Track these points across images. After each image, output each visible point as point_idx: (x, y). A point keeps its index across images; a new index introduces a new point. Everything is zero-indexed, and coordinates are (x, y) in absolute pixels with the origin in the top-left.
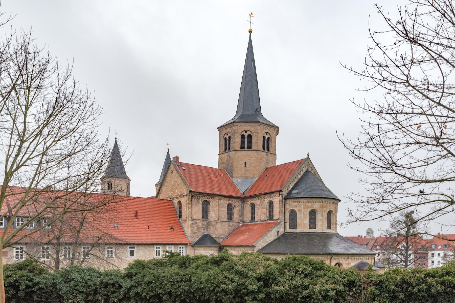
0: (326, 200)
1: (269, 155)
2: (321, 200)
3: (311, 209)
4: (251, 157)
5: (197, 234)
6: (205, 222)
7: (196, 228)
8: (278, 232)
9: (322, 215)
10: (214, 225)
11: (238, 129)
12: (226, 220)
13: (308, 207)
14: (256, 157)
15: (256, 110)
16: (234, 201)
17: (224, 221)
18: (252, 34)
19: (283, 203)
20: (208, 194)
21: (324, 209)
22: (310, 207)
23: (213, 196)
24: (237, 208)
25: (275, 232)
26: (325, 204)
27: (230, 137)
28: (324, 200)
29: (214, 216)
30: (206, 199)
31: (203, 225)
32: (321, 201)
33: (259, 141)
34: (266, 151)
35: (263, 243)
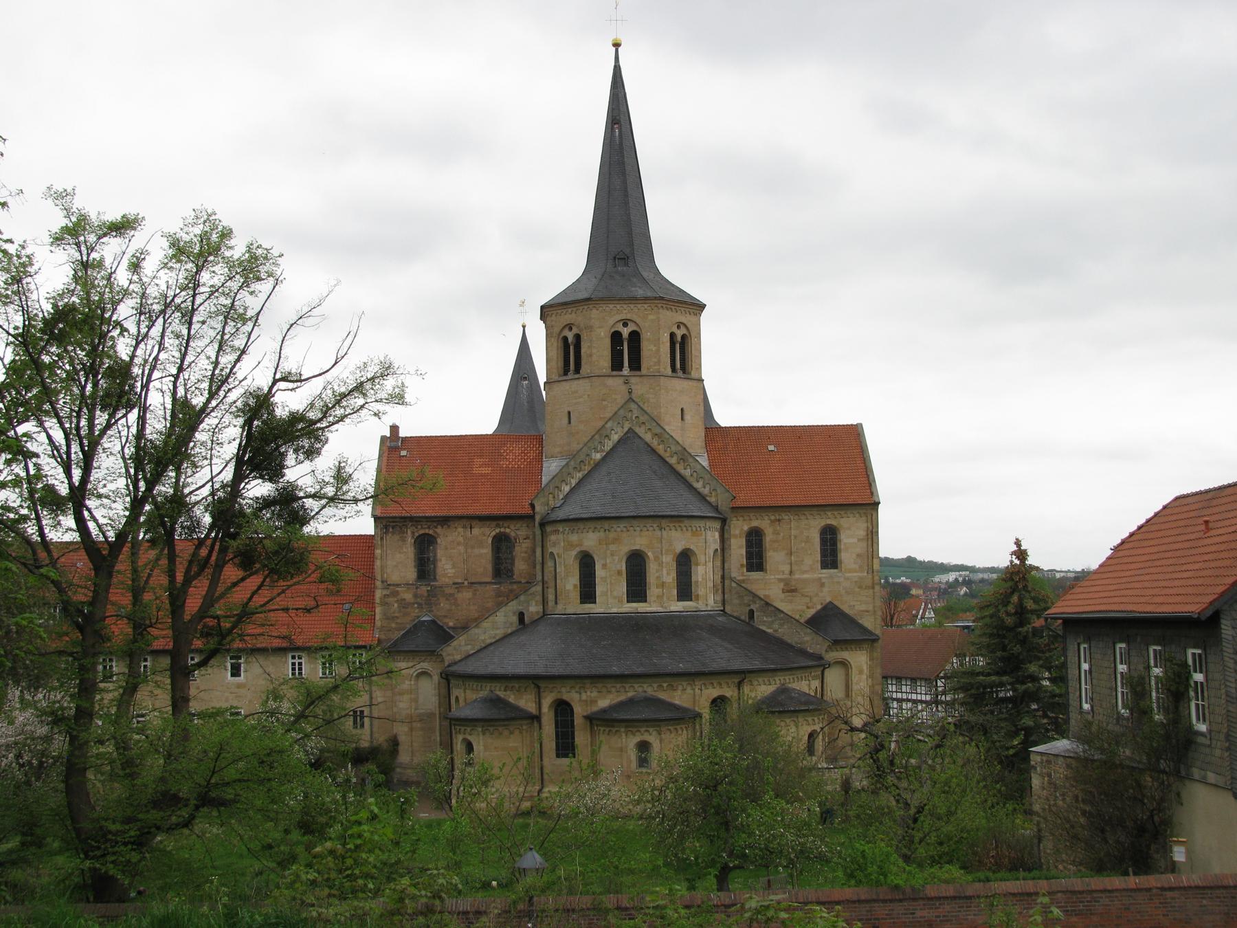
0: (615, 524)
1: (633, 380)
2: (598, 524)
3: (578, 549)
4: (580, 397)
5: (399, 621)
6: (424, 590)
7: (396, 605)
8: (521, 616)
9: (604, 566)
10: (452, 595)
11: (553, 323)
12: (489, 580)
13: (571, 546)
14: (589, 395)
15: (615, 258)
16: (512, 527)
17: (480, 583)
18: (620, 49)
19: (539, 537)
20: (428, 519)
21: (613, 547)
22: (577, 546)
23: (445, 521)
24: (524, 545)
25: (511, 614)
26: (612, 535)
27: (578, 337)
28: (606, 525)
29: (451, 572)
30: (427, 531)
31: (416, 596)
32: (599, 527)
33: (594, 351)
34: (626, 371)
35: (466, 645)
